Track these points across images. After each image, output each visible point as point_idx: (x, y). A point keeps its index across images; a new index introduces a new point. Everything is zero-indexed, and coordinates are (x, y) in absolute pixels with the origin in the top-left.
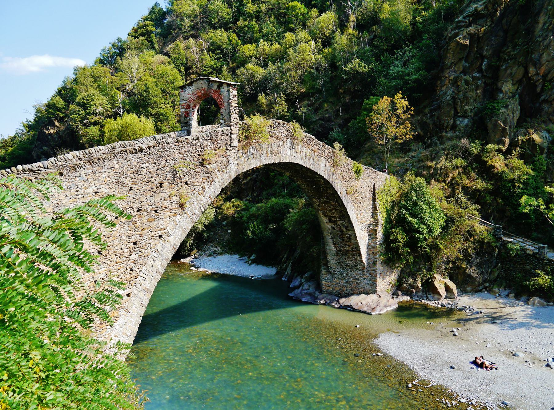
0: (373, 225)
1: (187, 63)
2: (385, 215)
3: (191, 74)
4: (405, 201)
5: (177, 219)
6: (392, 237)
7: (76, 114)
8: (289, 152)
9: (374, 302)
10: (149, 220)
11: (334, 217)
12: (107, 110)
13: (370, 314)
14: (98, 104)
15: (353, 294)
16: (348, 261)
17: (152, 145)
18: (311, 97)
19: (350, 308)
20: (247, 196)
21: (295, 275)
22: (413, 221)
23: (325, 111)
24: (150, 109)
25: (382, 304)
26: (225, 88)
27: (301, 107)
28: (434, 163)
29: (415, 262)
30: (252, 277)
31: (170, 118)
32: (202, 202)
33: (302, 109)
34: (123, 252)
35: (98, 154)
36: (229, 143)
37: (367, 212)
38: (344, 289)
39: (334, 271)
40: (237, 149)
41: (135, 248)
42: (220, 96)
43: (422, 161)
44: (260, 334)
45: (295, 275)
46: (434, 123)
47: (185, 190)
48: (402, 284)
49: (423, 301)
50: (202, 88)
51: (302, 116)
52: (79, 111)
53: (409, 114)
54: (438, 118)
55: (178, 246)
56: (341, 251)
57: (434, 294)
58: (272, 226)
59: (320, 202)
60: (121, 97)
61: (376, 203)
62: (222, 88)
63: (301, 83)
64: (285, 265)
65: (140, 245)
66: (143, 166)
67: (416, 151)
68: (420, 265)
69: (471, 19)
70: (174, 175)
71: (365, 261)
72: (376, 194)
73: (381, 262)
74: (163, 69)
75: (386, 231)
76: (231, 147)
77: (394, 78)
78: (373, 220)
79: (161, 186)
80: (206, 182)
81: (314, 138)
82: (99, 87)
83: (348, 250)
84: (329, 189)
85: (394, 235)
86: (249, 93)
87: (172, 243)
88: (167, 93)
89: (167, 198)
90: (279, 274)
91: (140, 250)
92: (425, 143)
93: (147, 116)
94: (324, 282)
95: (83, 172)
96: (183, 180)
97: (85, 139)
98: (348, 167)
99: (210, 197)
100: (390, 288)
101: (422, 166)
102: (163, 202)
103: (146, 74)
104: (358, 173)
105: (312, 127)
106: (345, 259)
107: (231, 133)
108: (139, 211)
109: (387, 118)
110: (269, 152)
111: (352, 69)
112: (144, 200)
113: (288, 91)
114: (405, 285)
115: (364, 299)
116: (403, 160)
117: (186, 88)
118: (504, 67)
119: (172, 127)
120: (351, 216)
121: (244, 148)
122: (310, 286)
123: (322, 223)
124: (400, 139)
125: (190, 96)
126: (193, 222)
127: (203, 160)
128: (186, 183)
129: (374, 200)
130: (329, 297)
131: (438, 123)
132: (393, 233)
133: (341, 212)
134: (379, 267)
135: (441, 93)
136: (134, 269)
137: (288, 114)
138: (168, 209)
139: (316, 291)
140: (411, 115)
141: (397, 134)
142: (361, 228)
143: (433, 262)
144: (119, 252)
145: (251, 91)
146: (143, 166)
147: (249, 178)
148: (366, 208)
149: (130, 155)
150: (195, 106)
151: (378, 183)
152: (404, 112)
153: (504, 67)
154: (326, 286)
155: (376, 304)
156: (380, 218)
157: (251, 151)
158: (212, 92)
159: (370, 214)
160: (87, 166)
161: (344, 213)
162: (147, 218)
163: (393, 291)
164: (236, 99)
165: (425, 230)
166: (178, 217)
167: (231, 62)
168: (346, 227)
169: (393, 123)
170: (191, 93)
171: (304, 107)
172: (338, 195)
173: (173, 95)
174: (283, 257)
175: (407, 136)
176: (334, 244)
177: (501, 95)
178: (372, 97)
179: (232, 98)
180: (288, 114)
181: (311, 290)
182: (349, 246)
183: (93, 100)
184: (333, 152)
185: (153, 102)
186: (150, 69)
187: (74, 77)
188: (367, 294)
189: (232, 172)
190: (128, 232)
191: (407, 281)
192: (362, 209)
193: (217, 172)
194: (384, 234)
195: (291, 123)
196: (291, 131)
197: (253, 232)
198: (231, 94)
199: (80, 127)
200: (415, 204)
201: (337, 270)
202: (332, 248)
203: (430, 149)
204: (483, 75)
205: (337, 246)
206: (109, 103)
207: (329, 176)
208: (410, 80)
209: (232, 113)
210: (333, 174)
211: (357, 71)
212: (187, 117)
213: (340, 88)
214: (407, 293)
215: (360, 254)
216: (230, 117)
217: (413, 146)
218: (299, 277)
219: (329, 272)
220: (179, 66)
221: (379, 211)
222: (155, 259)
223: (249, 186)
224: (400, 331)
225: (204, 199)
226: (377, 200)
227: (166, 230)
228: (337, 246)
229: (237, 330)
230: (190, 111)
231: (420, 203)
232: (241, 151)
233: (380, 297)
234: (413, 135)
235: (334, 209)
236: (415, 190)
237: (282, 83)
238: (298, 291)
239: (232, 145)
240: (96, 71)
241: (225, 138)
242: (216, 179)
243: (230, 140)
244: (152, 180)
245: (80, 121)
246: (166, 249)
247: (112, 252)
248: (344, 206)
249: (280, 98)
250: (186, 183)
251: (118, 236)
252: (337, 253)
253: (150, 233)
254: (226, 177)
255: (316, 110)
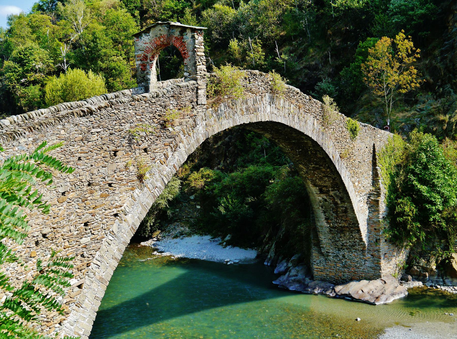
0: (374, 194)
1: (142, 6)
2: (388, 182)
3: (147, 18)
4: (413, 164)
5: (135, 194)
6: (398, 209)
7: (12, 72)
8: (268, 109)
9: (378, 289)
10: (101, 196)
11: (326, 187)
12: (48, 66)
13: (373, 304)
14: (37, 59)
15: (352, 280)
16: (345, 240)
17: (103, 105)
18: (293, 41)
19: (348, 298)
20: (219, 164)
21: (280, 258)
22: (423, 188)
23: (311, 57)
24: (99, 62)
25: (388, 292)
26: (189, 34)
27: (281, 54)
28: (448, 116)
29: (427, 240)
30: (227, 262)
31: (124, 72)
32: (165, 173)
33: (283, 56)
34: (72, 235)
35: (39, 118)
36: (195, 100)
37: (366, 178)
38: (340, 274)
39: (327, 252)
40: (205, 107)
41: (86, 230)
42: (183, 44)
43: (433, 114)
44: (239, 331)
45: (280, 258)
46: (447, 68)
47: (145, 159)
48: (412, 267)
49: (439, 287)
50: (161, 35)
51: (283, 64)
52: (16, 68)
53: (415, 57)
54: (451, 61)
55: (138, 226)
56: (336, 227)
57: (452, 277)
58: (250, 200)
59: (308, 168)
60: (64, 49)
61: (377, 167)
62: (185, 34)
63: (280, 24)
64: (267, 246)
65: (92, 226)
66: (93, 130)
67: (424, 102)
68: (433, 243)
70: (130, 140)
71: (365, 239)
72: (377, 157)
73: (386, 241)
74: (114, 13)
75: (390, 202)
76: (197, 104)
77: (396, 14)
78: (372, 188)
79: (115, 155)
80: (169, 148)
81: (298, 90)
82: (38, 38)
83: (344, 227)
84: (318, 153)
85: (401, 207)
86: (217, 39)
87: (131, 223)
88: (120, 43)
89: (123, 169)
90: (261, 257)
91: (93, 232)
92: (436, 93)
93: (95, 71)
94: (315, 266)
95: (22, 140)
96: (141, 147)
97: (23, 102)
98: (341, 125)
99: (174, 166)
100: (397, 272)
101: (433, 121)
102: (119, 173)
103: (94, 21)
104: (354, 131)
105: (295, 77)
106: (341, 237)
107: (197, 89)
108: (89, 185)
109: (387, 64)
110: (244, 110)
111: (342, 5)
112: (95, 172)
113: (265, 35)
114: (415, 267)
115: (366, 286)
116: (409, 114)
117: (142, 36)
119: (127, 84)
120: (346, 185)
121: (214, 105)
122: (298, 271)
123: (311, 194)
124: (404, 88)
125: (147, 45)
126: (154, 197)
127: (165, 122)
128: (145, 150)
129: (374, 164)
130: (322, 284)
131: (451, 67)
132: (399, 204)
133: (334, 180)
134: (383, 246)
135: (454, 30)
136: (85, 255)
137: (266, 63)
138: (124, 182)
139: (306, 277)
140: (417, 59)
141: (401, 83)
142: (359, 199)
143: (450, 239)
144: (68, 234)
145: (219, 36)
146: (93, 130)
147: (220, 143)
148: (364, 174)
149: (78, 119)
150: (153, 57)
151: (378, 143)
152: (409, 56)
154: (318, 271)
155: (381, 292)
156: (382, 186)
157: (223, 108)
158: (174, 39)
159: (370, 181)
160: (27, 133)
161: (338, 181)
162: (100, 193)
163: (400, 276)
164: (203, 47)
165: (439, 201)
166: (137, 191)
167: (194, 3)
168: (341, 199)
169: (395, 69)
170: (148, 41)
171: (285, 54)
172: (330, 159)
173: (127, 45)
174: (265, 236)
175: (413, 85)
176: (327, 219)
178: (369, 38)
179: (197, 46)
180: (266, 63)
181: (300, 276)
182: (345, 221)
183: (31, 54)
184: (322, 107)
185: (103, 54)
186: (98, 15)
187: (9, 27)
188: (369, 279)
189: (200, 135)
190: (78, 210)
191: (418, 263)
192: (360, 175)
193: (182, 136)
194: (388, 206)
195: (270, 73)
196: (270, 83)
197: (226, 208)
198: (196, 41)
199: (17, 87)
200: (425, 168)
201: (331, 251)
202: (325, 224)
203: (442, 99)
205: (330, 221)
206: (51, 57)
207: (318, 136)
208: (415, 16)
209: (198, 64)
210: (323, 134)
211: (348, 7)
212: (144, 71)
213: (328, 29)
214: (418, 277)
215: (359, 231)
216: (196, 69)
217: (421, 97)
218: (284, 261)
219: (322, 254)
220: (133, 9)
221: (381, 178)
222: (110, 242)
223: (221, 152)
224: (412, 324)
225: (167, 169)
226: (378, 164)
227: (122, 208)
228: (330, 221)
229: (211, 327)
230: (148, 63)
231: (431, 166)
232: (210, 109)
233: (385, 283)
234: (420, 83)
235: (324, 176)
236: (425, 151)
237: (257, 26)
238: (284, 278)
239: (199, 103)
240: (34, 20)
241: (190, 95)
242: (181, 145)
243: (197, 97)
244: (105, 147)
245: (17, 80)
246: (123, 230)
247: (60, 235)
248: (338, 172)
249: (256, 43)
250: (145, 150)
251: (65, 215)
252: (331, 231)
253: (104, 211)
254: (193, 141)
255: (300, 57)
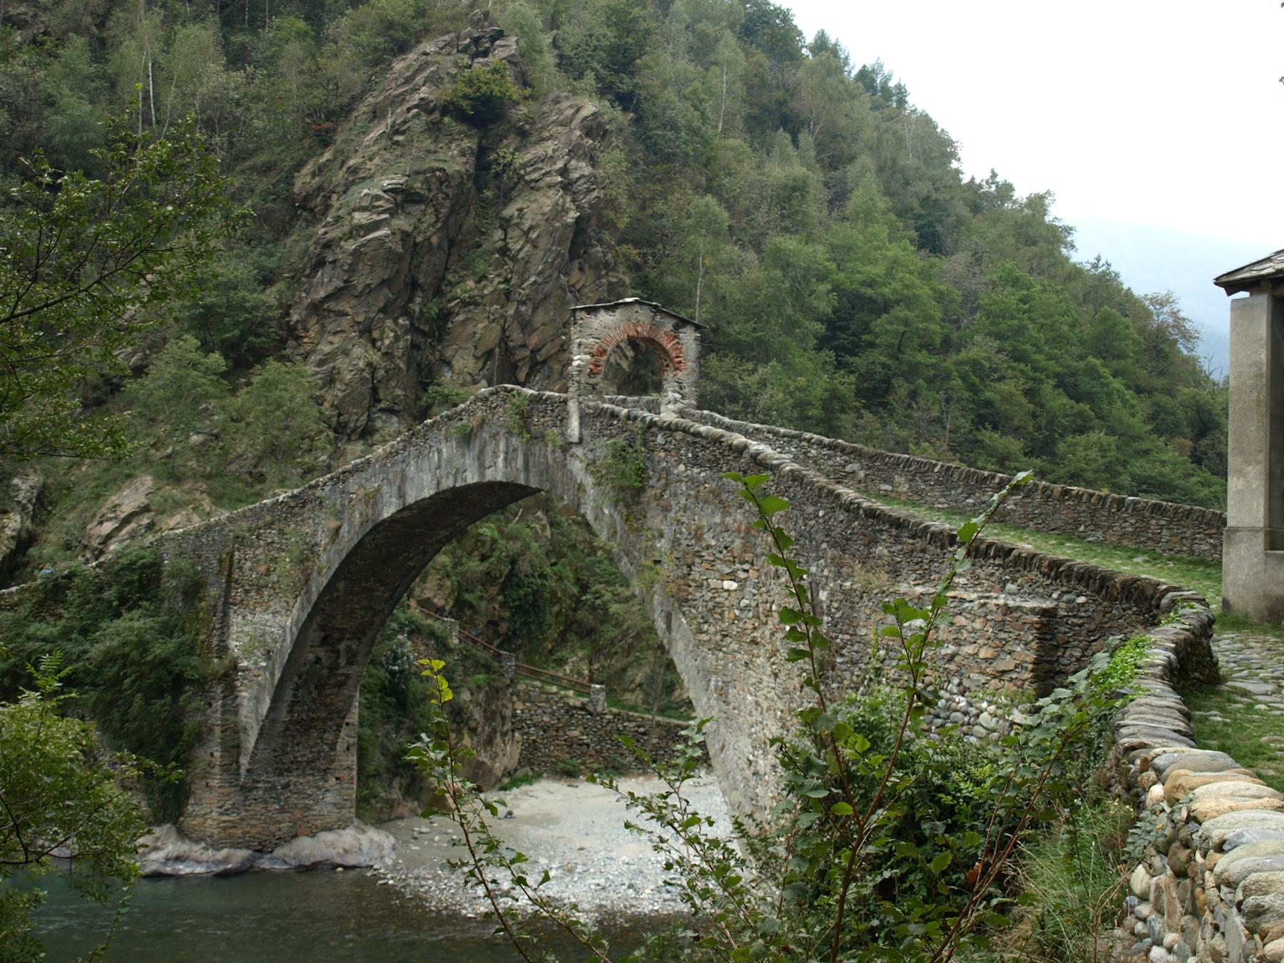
38: (273, 828)
69: (399, 198)
106: (298, 744)
118: (461, 318)
131: (335, 419)
135: (327, 349)
153: (461, 318)
177: (449, 375)
204: (412, 324)
252: (287, 729)
